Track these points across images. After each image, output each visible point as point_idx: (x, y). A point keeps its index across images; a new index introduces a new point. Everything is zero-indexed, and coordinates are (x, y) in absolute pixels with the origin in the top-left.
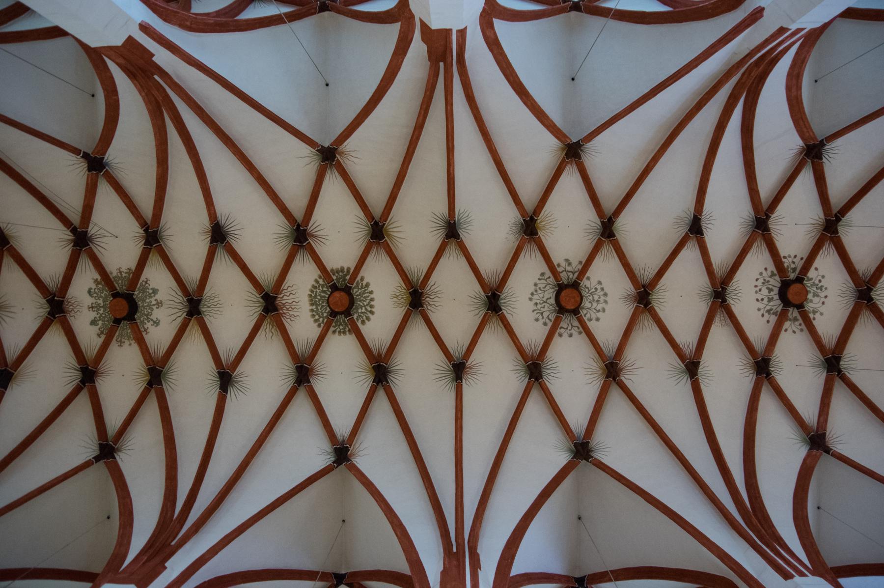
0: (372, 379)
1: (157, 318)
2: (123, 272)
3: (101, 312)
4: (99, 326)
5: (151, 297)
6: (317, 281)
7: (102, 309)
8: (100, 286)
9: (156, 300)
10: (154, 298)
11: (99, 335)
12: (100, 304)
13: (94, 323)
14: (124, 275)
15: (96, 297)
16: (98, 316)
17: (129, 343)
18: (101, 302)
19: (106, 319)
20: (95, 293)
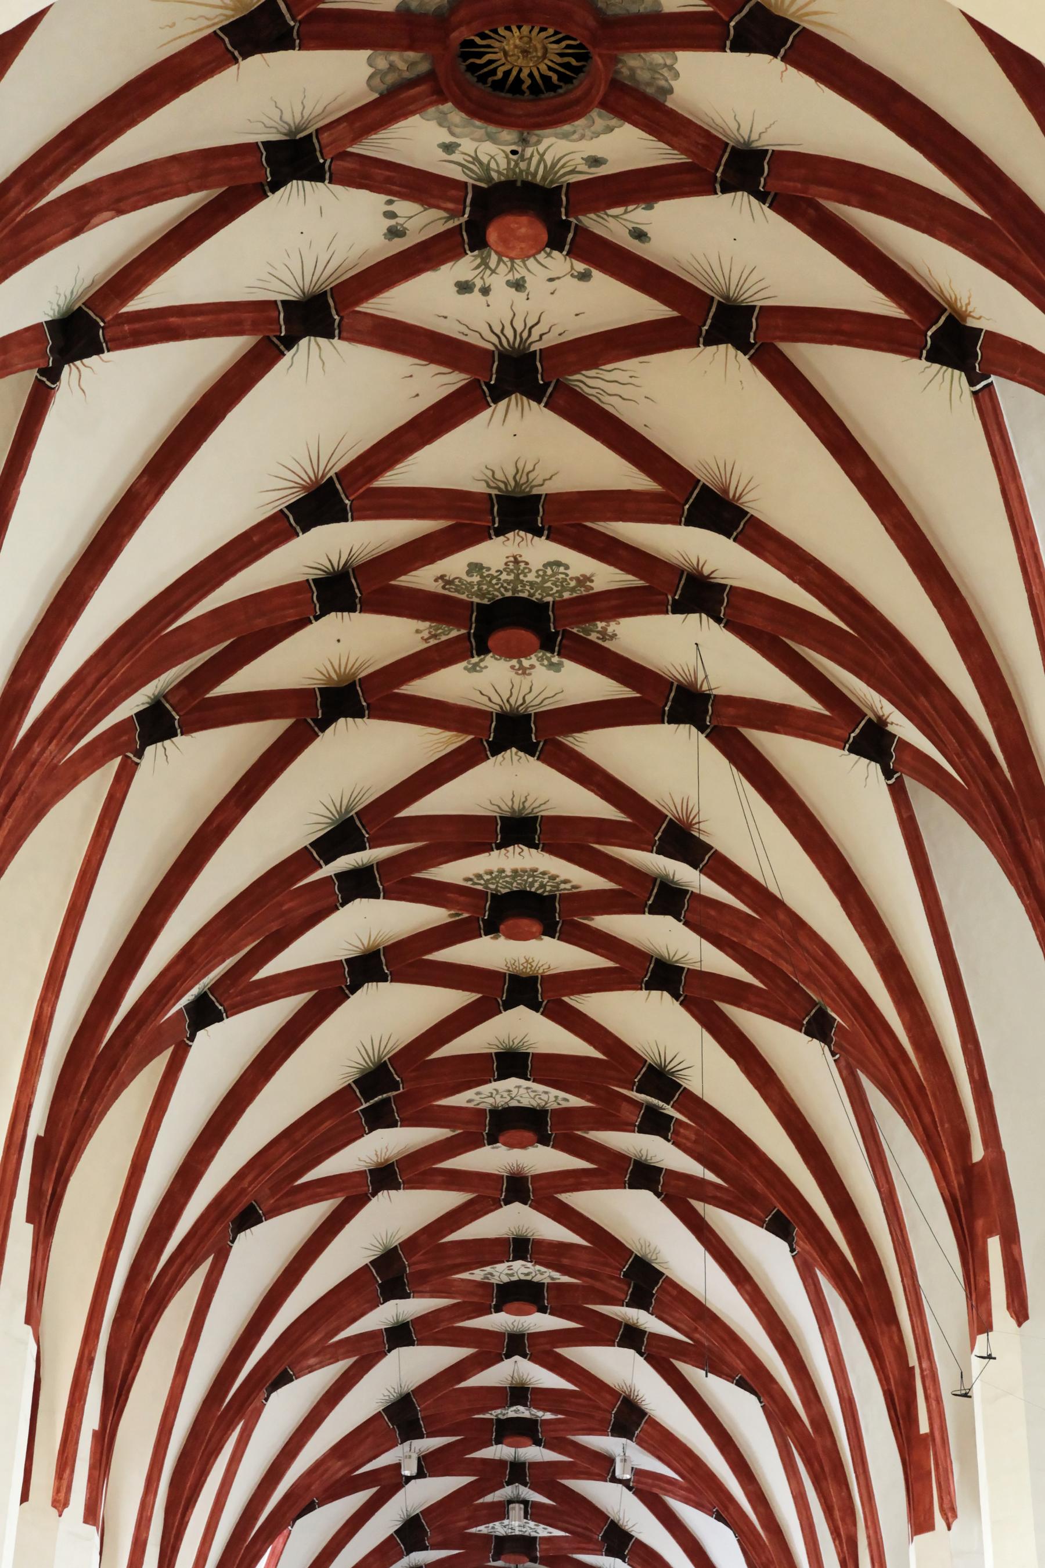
1: (486, 667)
2: (609, 626)
3: (504, 576)
4: (465, 577)
6: (566, 882)
7: (511, 577)
9: (532, 667)
10: (537, 664)
11: (442, 577)
12: (525, 576)
15: (545, 572)
16: (493, 572)
17: (421, 628)
18: (531, 577)
19: (485, 587)
20: (554, 574)
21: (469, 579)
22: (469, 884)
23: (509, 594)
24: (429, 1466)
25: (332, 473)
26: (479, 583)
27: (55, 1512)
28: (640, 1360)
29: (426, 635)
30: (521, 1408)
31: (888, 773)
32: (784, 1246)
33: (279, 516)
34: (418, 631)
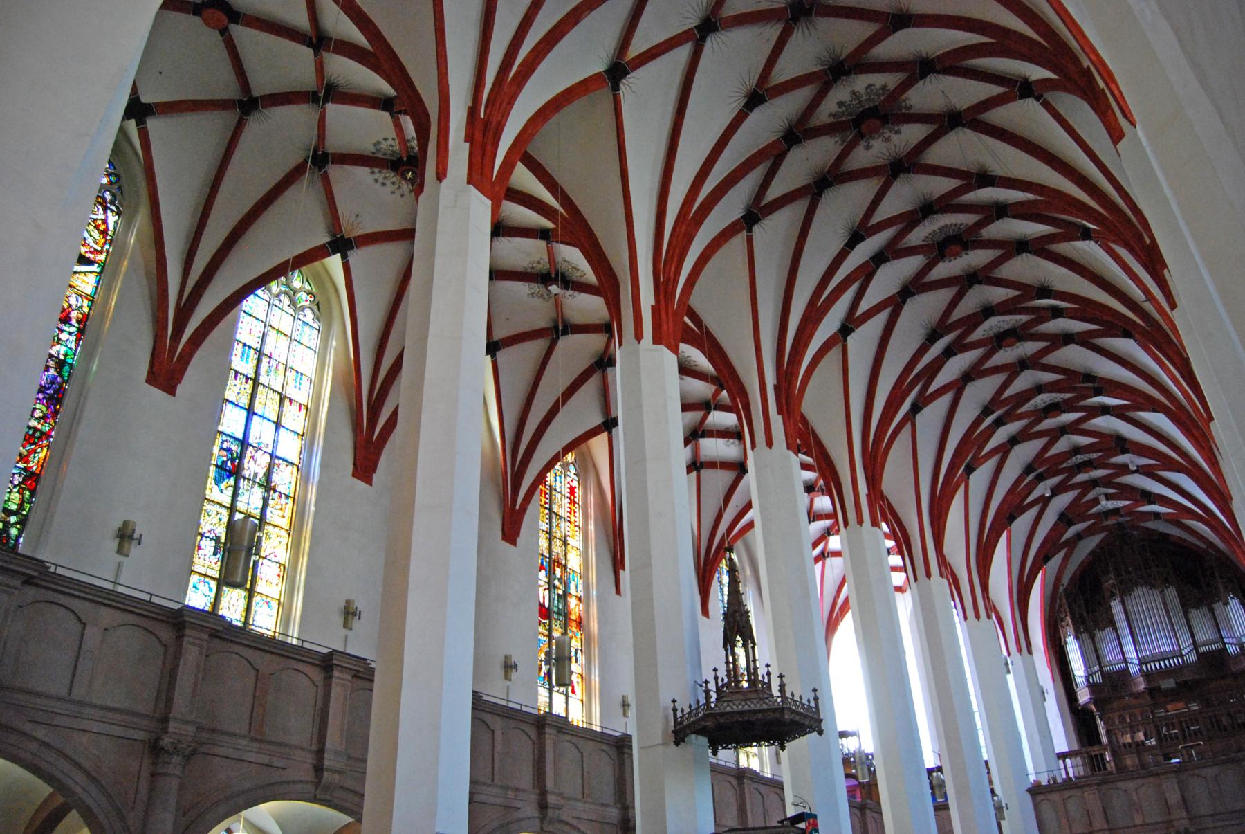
0: (897, 290)
3: (854, 102)
5: (890, 131)
6: (961, 224)
8: (881, 91)
9: (890, 137)
13: (840, 104)
14: (904, 104)
18: (864, 97)
20: (872, 91)
21: (841, 110)
22: (925, 243)
23: (861, 109)
24: (1056, 491)
25: (753, 87)
26: (847, 110)
27: (859, 526)
28: (1113, 419)
29: (840, 142)
30: (1079, 456)
31: (1038, 99)
32: (1132, 341)
33: (741, 111)
34: (836, 142)
